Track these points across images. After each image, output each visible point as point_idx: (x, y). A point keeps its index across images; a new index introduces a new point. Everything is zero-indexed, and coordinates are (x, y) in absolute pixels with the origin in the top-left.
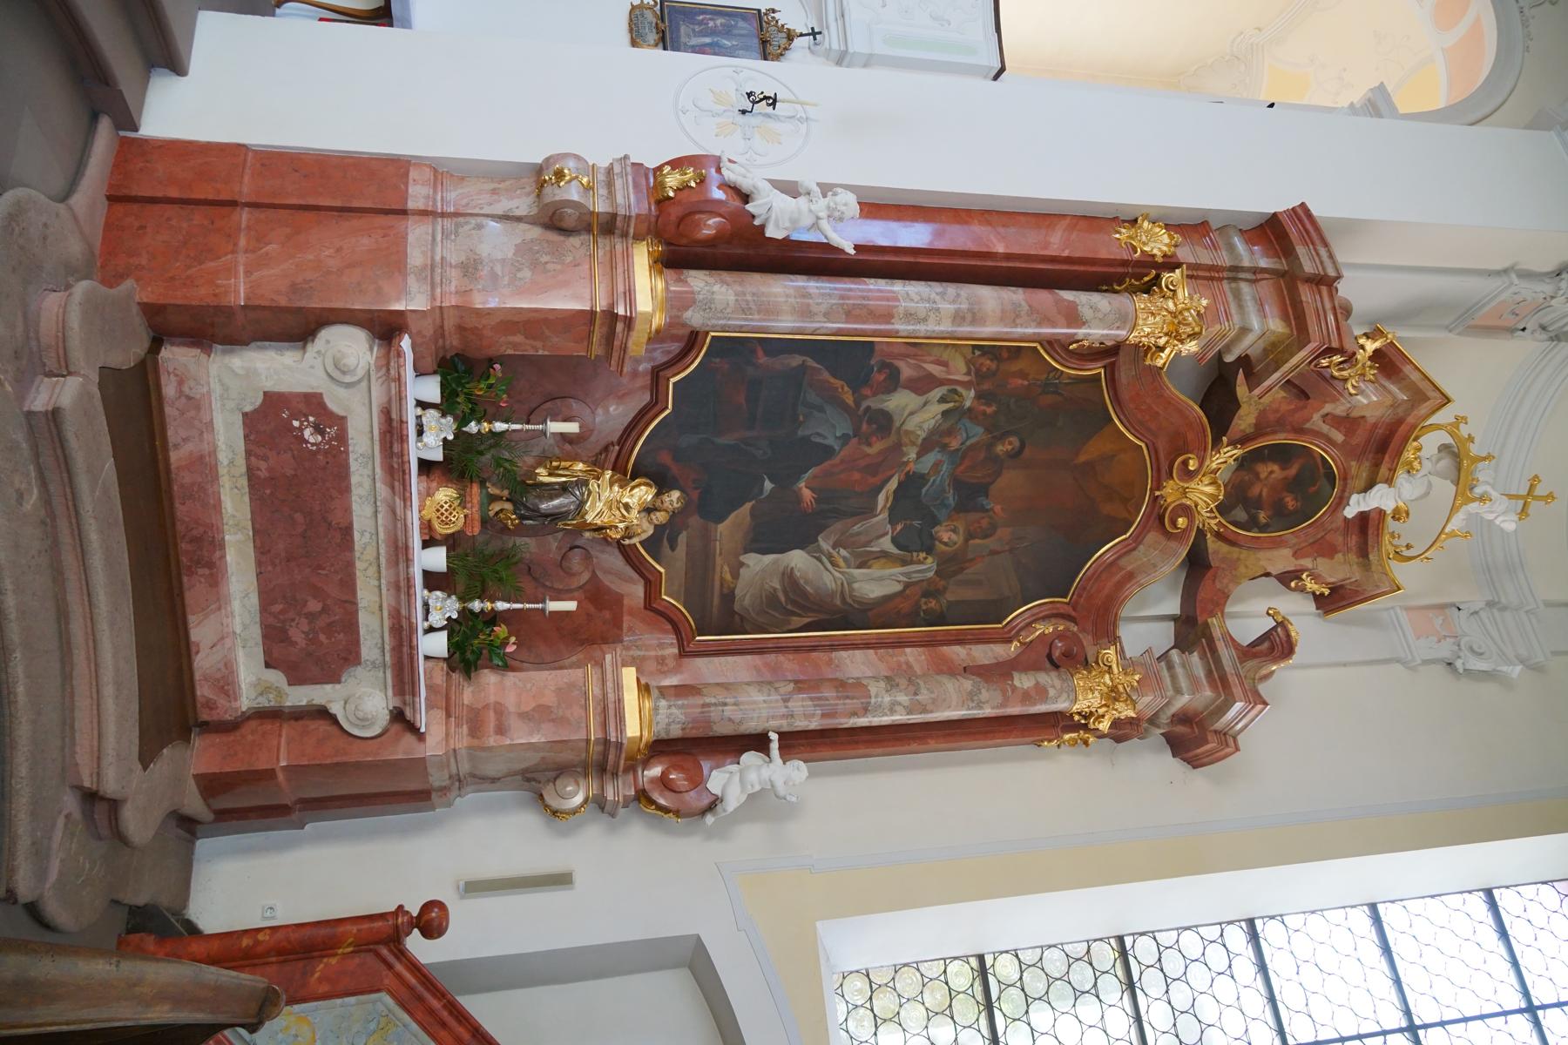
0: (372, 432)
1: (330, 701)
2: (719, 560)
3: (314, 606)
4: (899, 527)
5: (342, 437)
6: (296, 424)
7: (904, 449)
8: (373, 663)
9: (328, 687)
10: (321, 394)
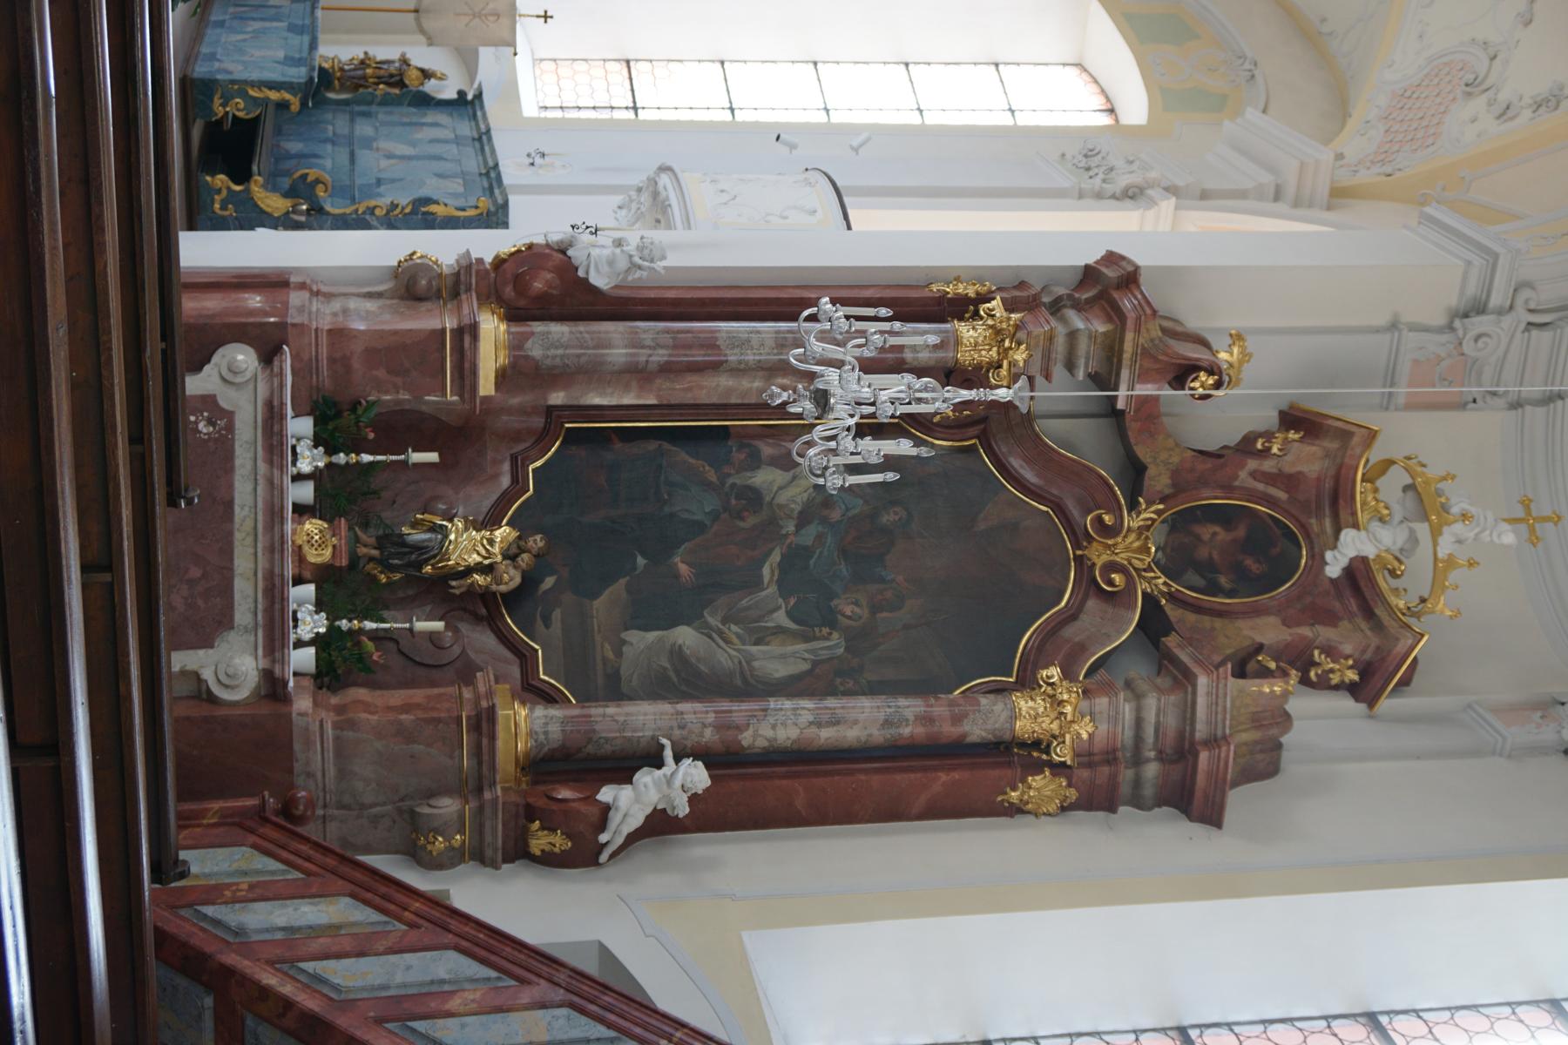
0: (256, 422)
1: (202, 667)
2: (598, 638)
3: (195, 572)
4: (792, 601)
5: (230, 428)
6: (192, 418)
7: (781, 523)
8: (246, 627)
9: (201, 652)
10: (215, 396)
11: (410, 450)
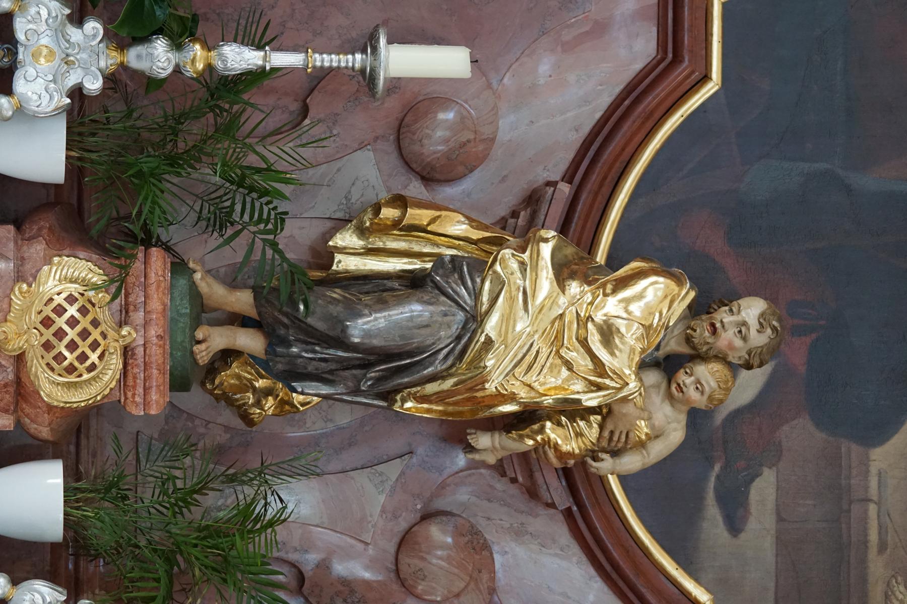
11: (383, 41)
